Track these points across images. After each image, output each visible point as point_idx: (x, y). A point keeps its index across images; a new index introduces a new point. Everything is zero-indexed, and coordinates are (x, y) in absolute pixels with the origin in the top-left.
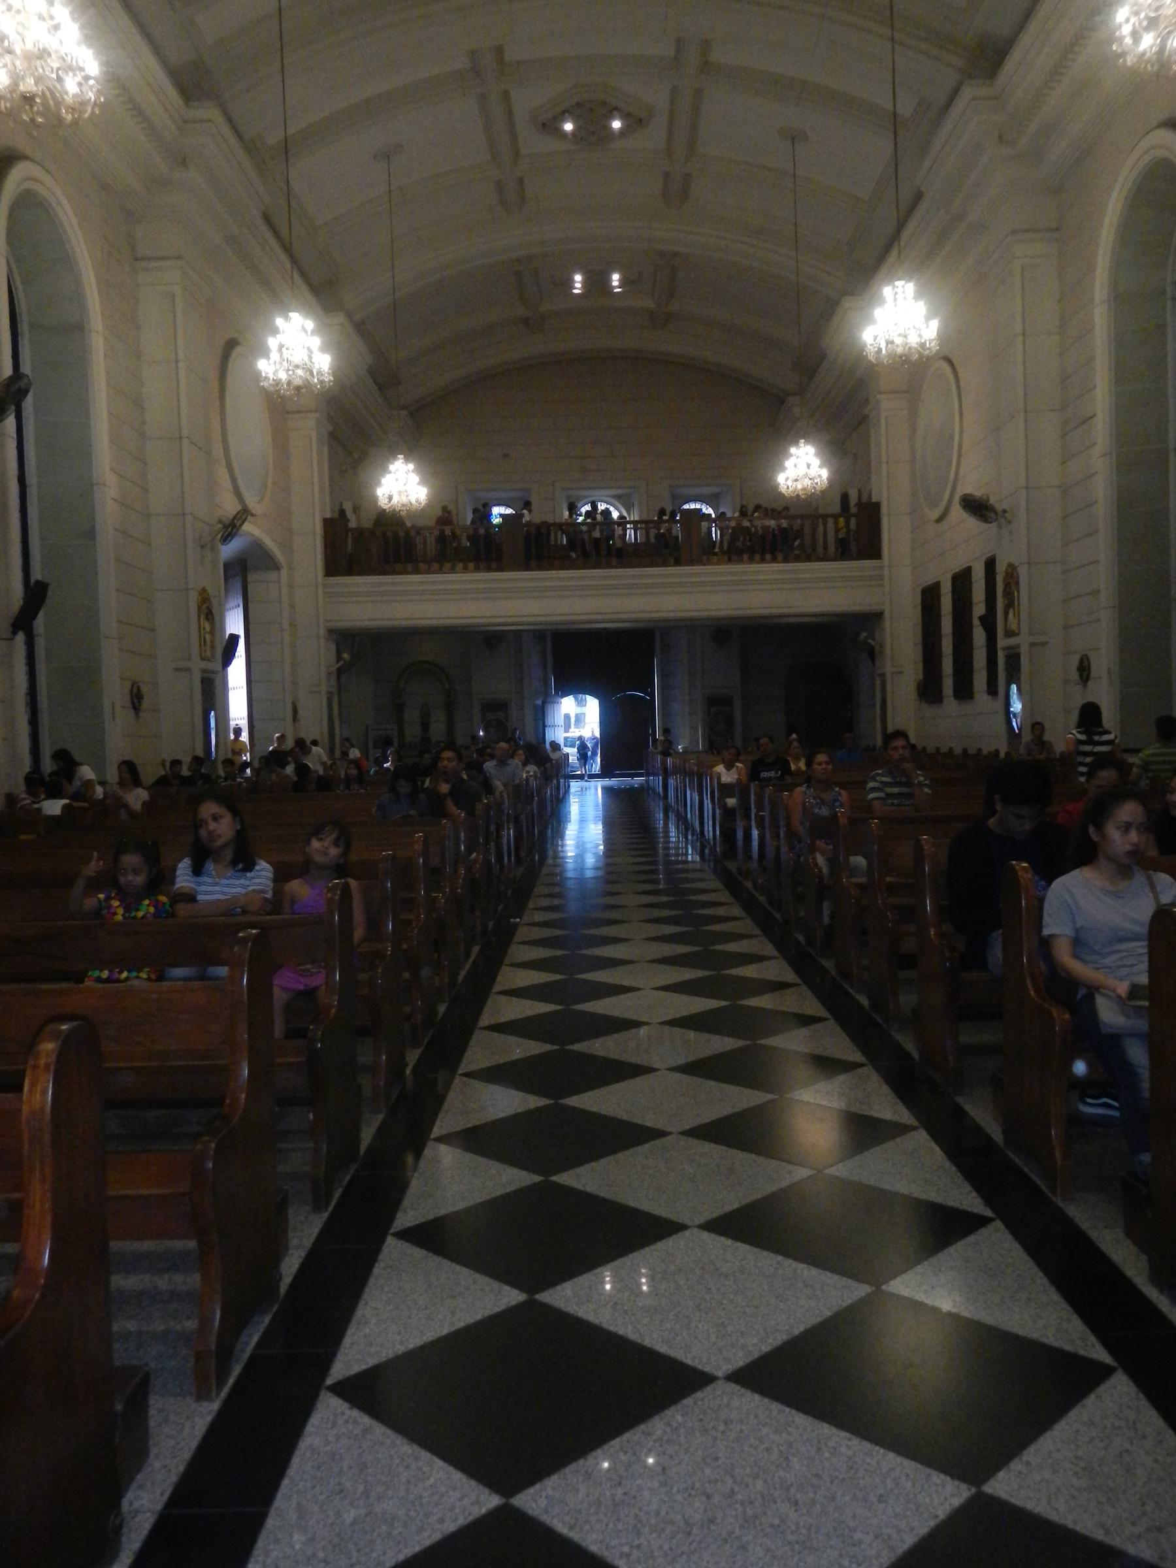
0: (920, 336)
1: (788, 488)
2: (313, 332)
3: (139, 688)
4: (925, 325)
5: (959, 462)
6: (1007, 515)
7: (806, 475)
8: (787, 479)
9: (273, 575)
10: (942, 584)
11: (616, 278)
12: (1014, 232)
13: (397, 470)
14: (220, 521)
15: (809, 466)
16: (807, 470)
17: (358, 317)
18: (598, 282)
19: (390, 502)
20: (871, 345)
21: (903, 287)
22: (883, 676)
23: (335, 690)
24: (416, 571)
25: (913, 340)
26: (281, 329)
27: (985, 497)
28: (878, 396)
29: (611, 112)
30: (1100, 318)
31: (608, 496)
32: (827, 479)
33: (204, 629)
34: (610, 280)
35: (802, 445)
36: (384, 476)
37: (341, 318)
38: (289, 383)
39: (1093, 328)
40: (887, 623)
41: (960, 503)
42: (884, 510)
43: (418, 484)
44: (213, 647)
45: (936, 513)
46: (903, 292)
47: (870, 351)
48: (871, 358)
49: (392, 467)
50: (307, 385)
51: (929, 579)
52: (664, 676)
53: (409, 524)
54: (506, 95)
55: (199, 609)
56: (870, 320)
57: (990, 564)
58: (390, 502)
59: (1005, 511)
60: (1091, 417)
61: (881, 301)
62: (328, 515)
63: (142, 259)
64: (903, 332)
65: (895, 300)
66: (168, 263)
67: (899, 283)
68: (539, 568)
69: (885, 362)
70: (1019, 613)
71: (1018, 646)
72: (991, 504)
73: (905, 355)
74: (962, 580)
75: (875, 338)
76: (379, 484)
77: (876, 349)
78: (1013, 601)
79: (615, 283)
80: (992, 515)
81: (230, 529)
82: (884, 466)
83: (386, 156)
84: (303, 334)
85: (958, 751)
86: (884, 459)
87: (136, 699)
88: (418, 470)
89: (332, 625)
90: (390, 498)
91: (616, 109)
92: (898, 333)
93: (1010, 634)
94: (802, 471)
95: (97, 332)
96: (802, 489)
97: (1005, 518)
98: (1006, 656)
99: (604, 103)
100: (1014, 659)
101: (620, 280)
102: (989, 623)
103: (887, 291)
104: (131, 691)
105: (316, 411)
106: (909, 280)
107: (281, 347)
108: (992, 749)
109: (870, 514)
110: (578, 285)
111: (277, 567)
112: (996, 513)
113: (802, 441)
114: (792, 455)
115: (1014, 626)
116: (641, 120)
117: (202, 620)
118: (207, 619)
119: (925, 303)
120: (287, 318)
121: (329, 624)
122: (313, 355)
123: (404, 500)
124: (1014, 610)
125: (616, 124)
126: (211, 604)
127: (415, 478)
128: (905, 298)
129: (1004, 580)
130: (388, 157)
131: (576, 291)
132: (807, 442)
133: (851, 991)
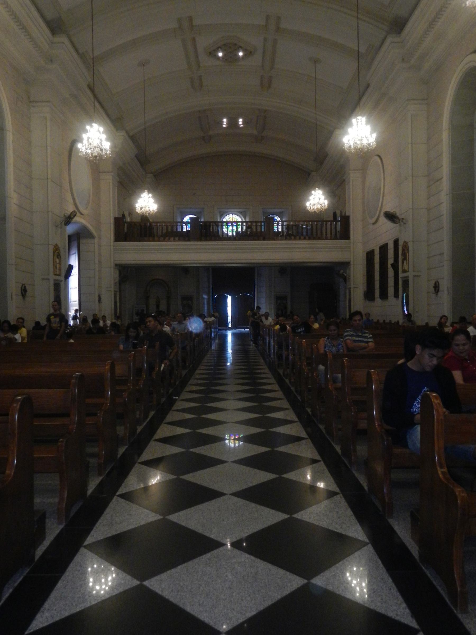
0: (368, 140)
1: (311, 208)
2: (103, 133)
3: (25, 287)
4: (370, 136)
5: (383, 199)
6: (404, 221)
7: (318, 203)
8: (310, 204)
10: (375, 250)
11: (241, 120)
12: (408, 100)
13: (144, 197)
14: (65, 216)
15: (319, 199)
16: (319, 201)
17: (131, 134)
18: (233, 123)
19: (141, 210)
20: (347, 144)
21: (361, 119)
22: (350, 288)
23: (118, 290)
24: (154, 240)
25: (365, 142)
26: (88, 130)
27: (395, 213)
28: (350, 172)
29: (238, 48)
30: (445, 136)
31: (236, 212)
32: (327, 205)
33: (56, 262)
34: (238, 122)
36: (139, 199)
37: (123, 133)
38: (92, 154)
39: (442, 140)
40: (352, 266)
41: (384, 215)
43: (154, 203)
44: (60, 269)
45: (374, 220)
46: (361, 121)
47: (346, 146)
48: (347, 150)
49: (142, 195)
50: (101, 156)
51: (369, 248)
53: (151, 221)
54: (194, 39)
55: (54, 253)
56: (346, 133)
57: (396, 242)
58: (141, 210)
59: (403, 219)
60: (440, 179)
61: (351, 125)
62: (117, 216)
63: (33, 102)
64: (361, 139)
65: (357, 124)
66: (43, 104)
67: (359, 118)
68: (206, 240)
69: (353, 151)
70: (409, 264)
71: (408, 277)
72: (397, 216)
73: (362, 149)
74: (384, 248)
75: (349, 141)
76: (137, 202)
77: (349, 146)
78: (406, 257)
79: (240, 123)
80: (398, 220)
81: (68, 220)
82: (351, 201)
83: (143, 64)
84: (99, 133)
85: (381, 321)
87: (24, 291)
88: (153, 197)
89: (118, 262)
90: (141, 208)
91: (241, 47)
92: (358, 139)
93: (404, 271)
94: (317, 201)
95: (9, 131)
96: (317, 209)
97: (403, 221)
98: (403, 281)
99: (235, 44)
100: (406, 282)
101: (242, 122)
102: (395, 266)
103: (354, 121)
104: (21, 288)
105: (112, 172)
106: (363, 116)
107: (89, 138)
108: (396, 321)
109: (346, 220)
110: (225, 123)
111: (93, 237)
112: (399, 220)
113: (317, 188)
114: (313, 194)
115: (406, 267)
116: (251, 52)
117: (55, 257)
118: (58, 258)
119: (371, 126)
120: (91, 126)
121: (115, 262)
122: (102, 142)
123: (147, 209)
124: (406, 261)
125: (241, 54)
126: (60, 251)
127: (152, 200)
128: (362, 124)
129: (402, 248)
130: (144, 65)
131: (224, 126)
132: (319, 188)
133: (333, 443)
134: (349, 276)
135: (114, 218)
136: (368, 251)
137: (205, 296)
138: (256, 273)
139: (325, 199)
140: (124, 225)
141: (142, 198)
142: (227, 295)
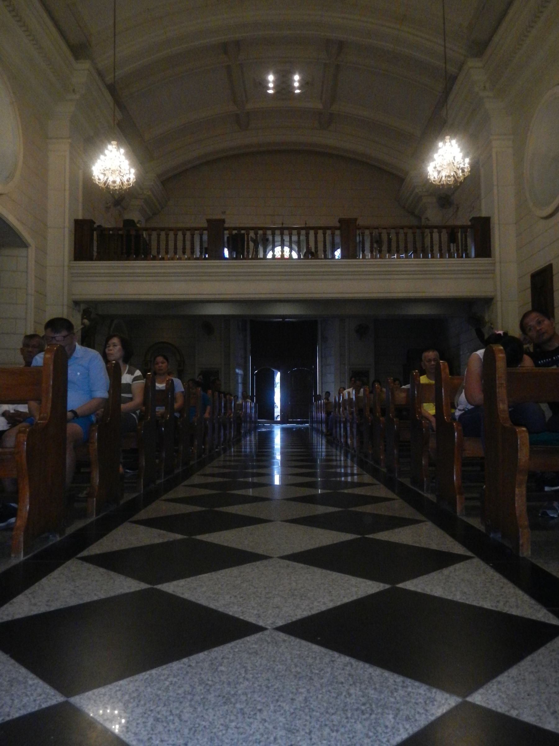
9: (22, 252)
10: (553, 264)
11: (297, 77)
17: (109, 79)
35: (448, 141)
42: (495, 220)
51: (539, 264)
52: (321, 358)
62: (80, 217)
79: (296, 84)
82: (495, 187)
86: (495, 183)
88: (127, 154)
89: (78, 298)
94: (449, 158)
110: (271, 85)
111: (24, 245)
113: (448, 137)
131: (271, 92)
134: (491, 324)
135: (73, 221)
136: (532, 273)
137: (239, 371)
138: (319, 337)
139: (464, 158)
140: (93, 235)
141: (105, 155)
142: (274, 370)
